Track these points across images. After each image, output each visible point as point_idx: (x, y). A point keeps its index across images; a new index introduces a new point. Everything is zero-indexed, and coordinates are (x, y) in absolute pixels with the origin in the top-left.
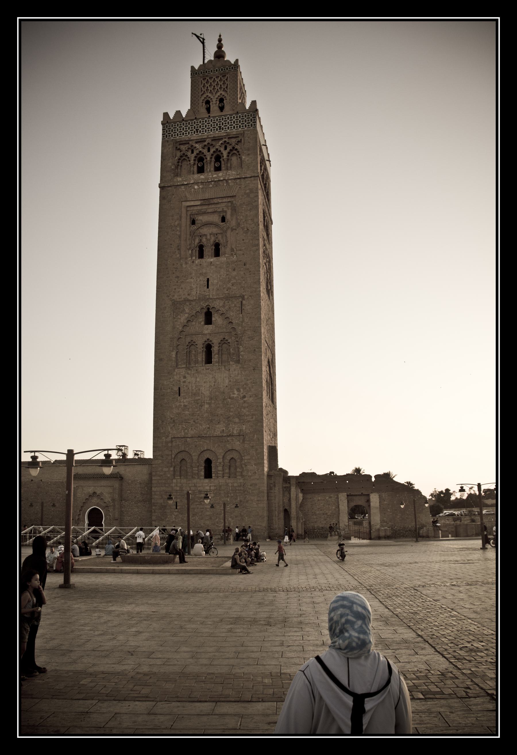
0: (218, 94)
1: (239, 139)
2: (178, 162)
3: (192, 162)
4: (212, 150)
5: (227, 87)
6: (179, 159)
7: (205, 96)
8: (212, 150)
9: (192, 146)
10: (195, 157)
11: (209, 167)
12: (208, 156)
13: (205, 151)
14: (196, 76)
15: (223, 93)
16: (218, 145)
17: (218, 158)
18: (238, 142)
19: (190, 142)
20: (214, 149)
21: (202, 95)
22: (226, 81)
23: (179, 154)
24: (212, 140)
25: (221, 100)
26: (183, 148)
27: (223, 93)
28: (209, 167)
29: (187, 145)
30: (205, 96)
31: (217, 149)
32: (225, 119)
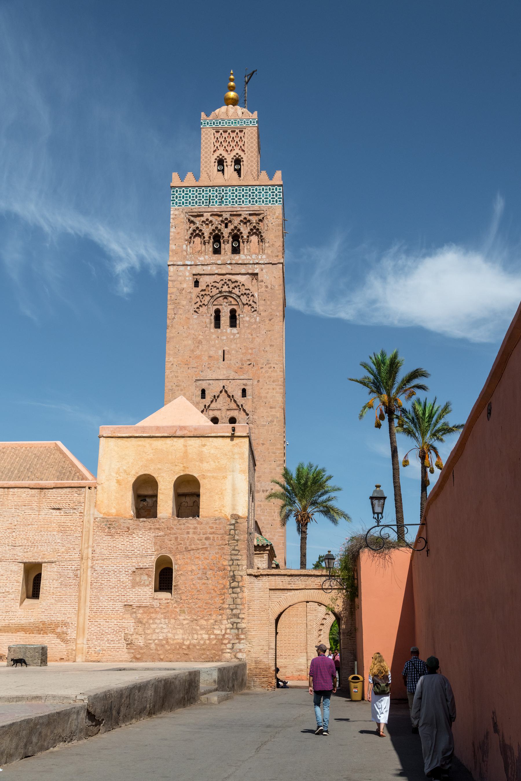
0: (234, 153)
1: (261, 217)
2: (190, 238)
3: (207, 238)
4: (231, 227)
5: (243, 145)
6: (192, 234)
7: (217, 154)
8: (231, 227)
9: (207, 220)
10: (211, 233)
11: (227, 248)
14: (208, 126)
15: (240, 153)
16: (236, 221)
17: (236, 237)
18: (260, 220)
19: (205, 214)
21: (214, 151)
22: (243, 138)
23: (193, 227)
24: (231, 215)
25: (238, 161)
26: (197, 220)
27: (240, 153)
28: (227, 248)
30: (217, 154)
31: (236, 227)
32: (246, 190)
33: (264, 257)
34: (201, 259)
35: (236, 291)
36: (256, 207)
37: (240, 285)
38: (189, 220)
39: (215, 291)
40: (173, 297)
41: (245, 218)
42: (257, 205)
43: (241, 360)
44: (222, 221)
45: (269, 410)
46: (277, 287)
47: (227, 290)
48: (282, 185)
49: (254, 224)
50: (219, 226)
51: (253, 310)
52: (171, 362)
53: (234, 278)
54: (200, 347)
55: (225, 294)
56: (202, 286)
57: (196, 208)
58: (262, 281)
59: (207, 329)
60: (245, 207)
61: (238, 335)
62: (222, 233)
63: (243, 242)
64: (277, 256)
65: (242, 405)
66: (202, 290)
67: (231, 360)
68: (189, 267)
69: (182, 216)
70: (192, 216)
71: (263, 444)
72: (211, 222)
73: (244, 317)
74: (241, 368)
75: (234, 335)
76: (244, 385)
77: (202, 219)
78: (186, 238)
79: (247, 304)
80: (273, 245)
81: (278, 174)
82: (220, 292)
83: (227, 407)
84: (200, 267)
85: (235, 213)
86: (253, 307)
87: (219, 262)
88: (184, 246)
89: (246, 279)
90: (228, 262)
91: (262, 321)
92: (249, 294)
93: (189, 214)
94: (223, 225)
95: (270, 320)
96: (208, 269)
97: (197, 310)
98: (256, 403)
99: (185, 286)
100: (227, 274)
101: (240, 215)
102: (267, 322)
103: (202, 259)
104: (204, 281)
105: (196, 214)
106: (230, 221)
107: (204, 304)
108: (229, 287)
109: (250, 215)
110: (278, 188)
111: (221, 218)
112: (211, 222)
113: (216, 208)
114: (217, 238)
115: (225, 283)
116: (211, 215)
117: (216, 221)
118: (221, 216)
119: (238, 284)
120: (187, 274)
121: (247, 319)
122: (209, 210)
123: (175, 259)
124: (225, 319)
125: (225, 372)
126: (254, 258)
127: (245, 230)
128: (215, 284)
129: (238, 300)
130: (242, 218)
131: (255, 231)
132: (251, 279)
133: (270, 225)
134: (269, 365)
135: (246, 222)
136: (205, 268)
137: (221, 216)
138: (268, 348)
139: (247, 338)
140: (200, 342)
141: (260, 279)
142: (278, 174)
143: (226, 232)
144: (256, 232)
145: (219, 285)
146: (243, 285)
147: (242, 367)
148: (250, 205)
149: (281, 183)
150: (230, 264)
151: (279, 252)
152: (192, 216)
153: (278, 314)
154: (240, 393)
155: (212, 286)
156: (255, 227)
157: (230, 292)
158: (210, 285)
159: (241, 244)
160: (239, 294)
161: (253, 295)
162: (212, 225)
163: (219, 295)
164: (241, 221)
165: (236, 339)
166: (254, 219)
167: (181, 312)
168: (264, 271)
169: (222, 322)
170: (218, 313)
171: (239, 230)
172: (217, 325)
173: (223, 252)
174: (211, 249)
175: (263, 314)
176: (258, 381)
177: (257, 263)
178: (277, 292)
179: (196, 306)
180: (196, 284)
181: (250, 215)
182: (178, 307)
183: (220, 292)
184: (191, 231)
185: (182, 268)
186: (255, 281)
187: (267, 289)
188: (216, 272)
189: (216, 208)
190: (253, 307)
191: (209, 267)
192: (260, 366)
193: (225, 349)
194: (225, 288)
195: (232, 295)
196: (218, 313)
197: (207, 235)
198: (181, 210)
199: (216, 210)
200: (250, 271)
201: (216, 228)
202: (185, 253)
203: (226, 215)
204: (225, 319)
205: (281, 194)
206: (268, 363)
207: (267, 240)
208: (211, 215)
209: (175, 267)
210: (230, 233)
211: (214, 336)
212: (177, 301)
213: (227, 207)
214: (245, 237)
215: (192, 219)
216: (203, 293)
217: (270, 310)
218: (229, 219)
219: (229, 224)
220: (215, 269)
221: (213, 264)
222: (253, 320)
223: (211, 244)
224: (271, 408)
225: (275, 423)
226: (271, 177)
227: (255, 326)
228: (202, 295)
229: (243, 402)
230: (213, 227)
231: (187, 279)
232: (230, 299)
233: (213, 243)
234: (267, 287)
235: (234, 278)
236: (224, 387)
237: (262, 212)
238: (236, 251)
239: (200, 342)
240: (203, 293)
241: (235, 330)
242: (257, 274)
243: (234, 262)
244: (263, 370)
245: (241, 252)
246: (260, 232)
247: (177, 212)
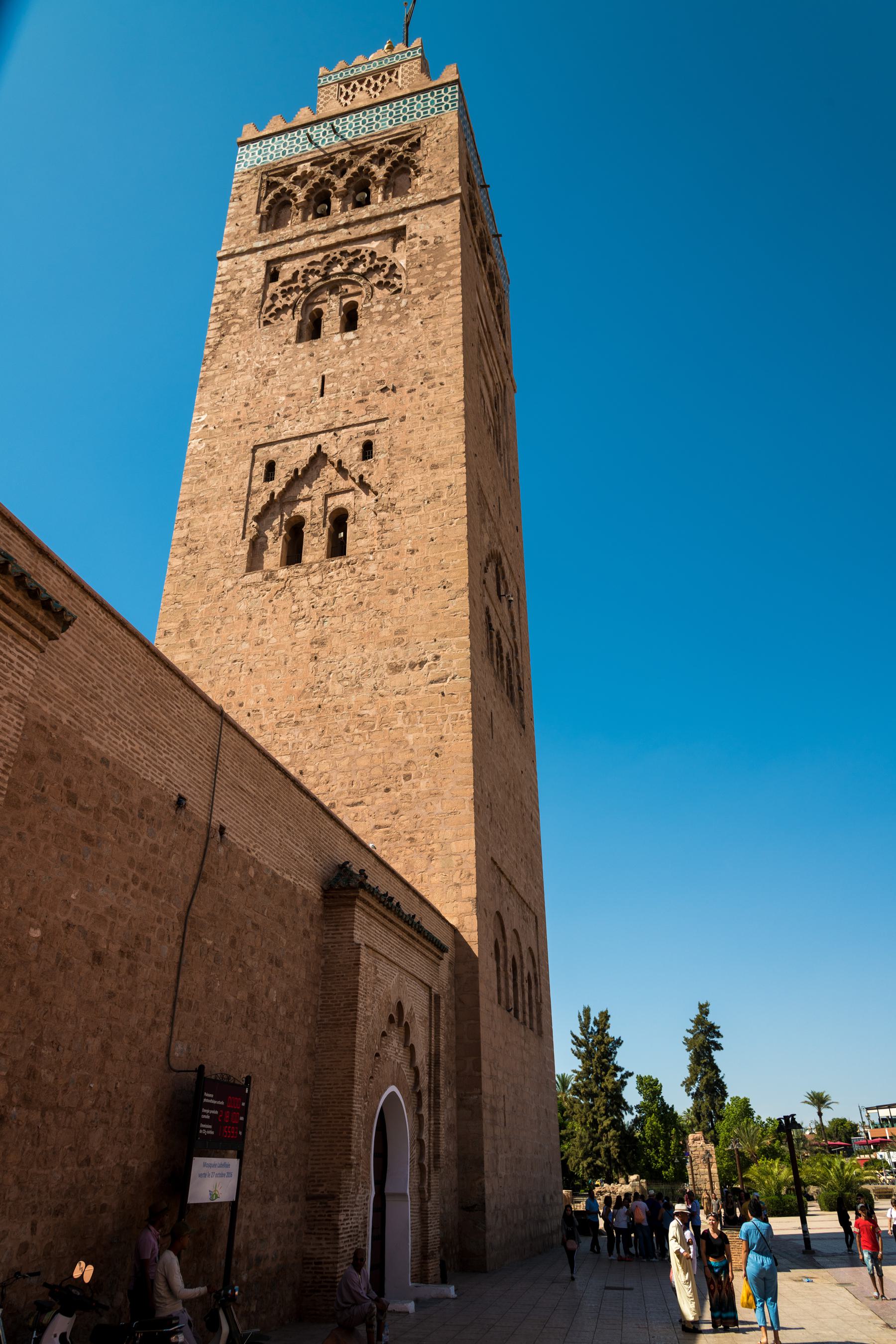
1: (415, 138)
13: (334, 178)
43: (363, 385)
45: (430, 472)
55: (334, 279)
58: (415, 236)
59: (288, 346)
61: (357, 342)
65: (361, 477)
66: (284, 284)
67: (338, 391)
71: (412, 552)
73: (372, 306)
74: (361, 401)
75: (349, 342)
76: (367, 433)
83: (326, 490)
95: (432, 298)
98: (397, 463)
102: (425, 301)
117: (322, 171)
121: (381, 307)
124: (331, 323)
125: (323, 418)
134: (431, 382)
138: (428, 351)
139: (377, 343)
145: (317, 267)
147: (366, 397)
153: (451, 283)
154: (357, 451)
164: (373, 157)
165: (353, 349)
175: (415, 291)
176: (403, 419)
181: (391, 142)
187: (424, 247)
192: (407, 388)
193: (325, 373)
201: (322, 180)
205: (457, 95)
206: (426, 379)
208: (312, 165)
210: (349, 181)
217: (432, 280)
224: (434, 467)
225: (445, 498)
227: (397, 316)
229: (365, 468)
236: (319, 447)
241: (350, 335)
244: (416, 395)
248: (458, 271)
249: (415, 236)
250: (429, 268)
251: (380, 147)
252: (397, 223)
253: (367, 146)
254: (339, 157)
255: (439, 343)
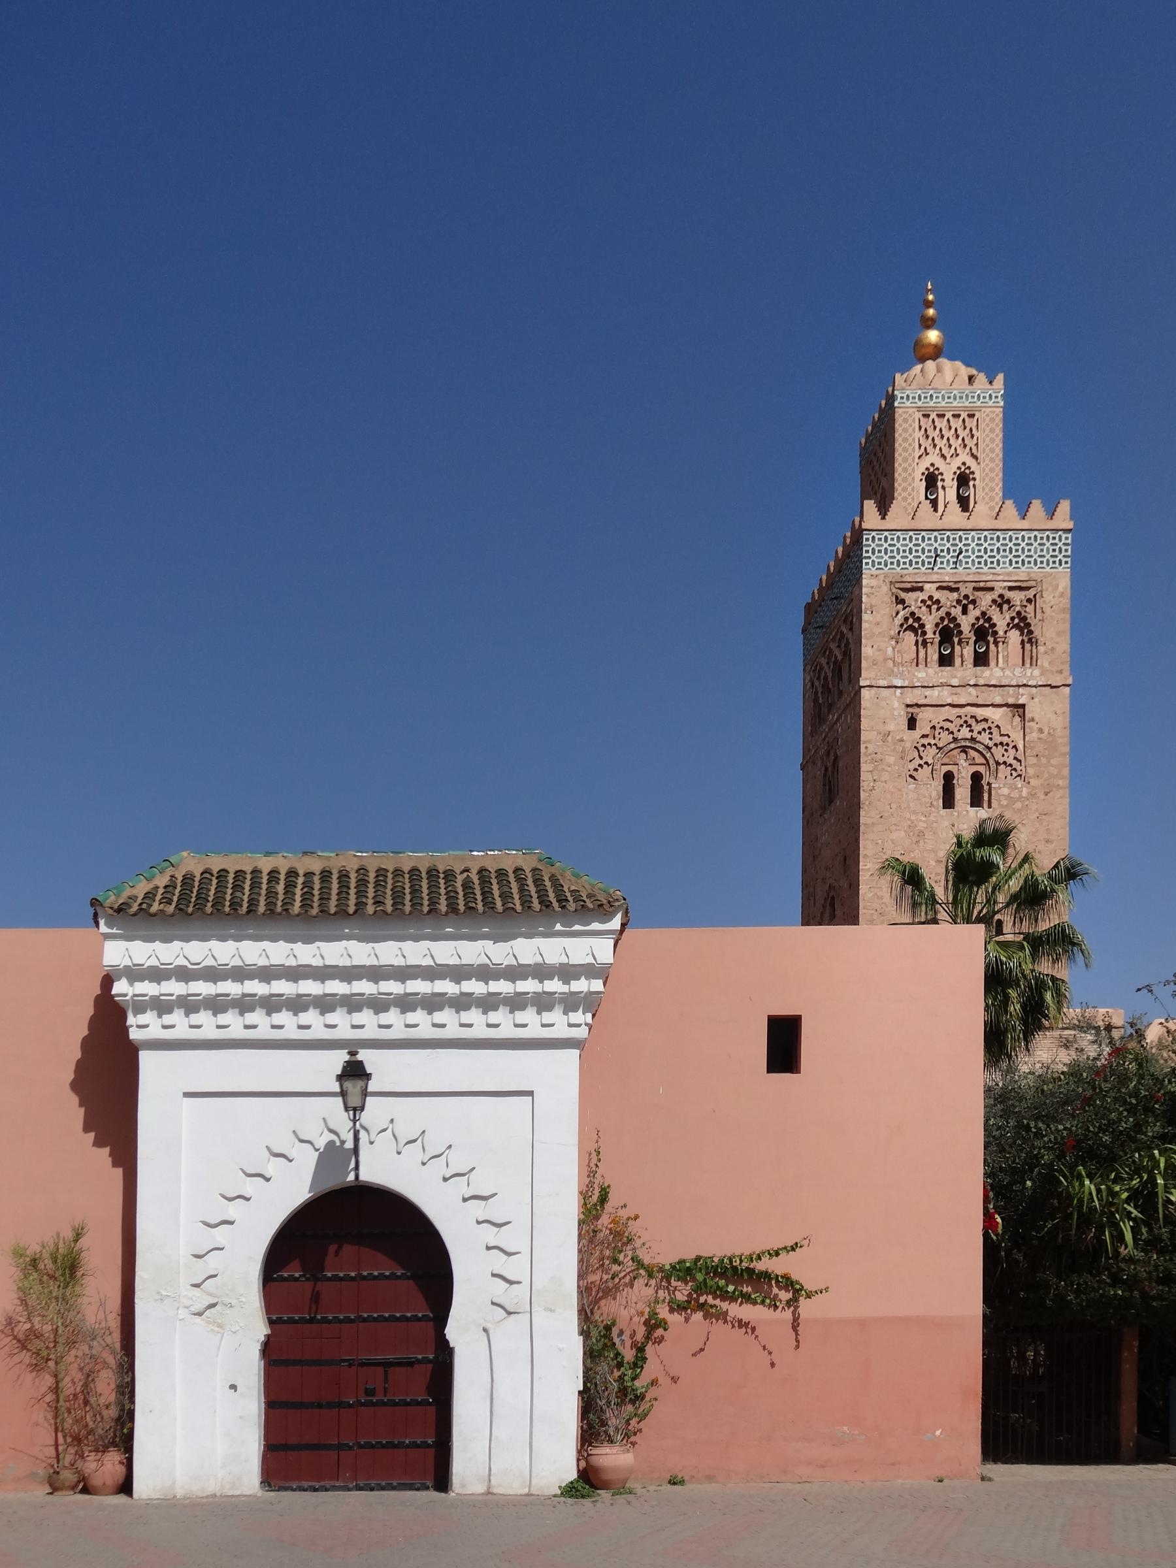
1: (1030, 594)
4: (974, 613)
6: (902, 625)
8: (974, 613)
9: (931, 598)
10: (937, 625)
12: (966, 628)
13: (957, 611)
16: (985, 599)
17: (984, 632)
18: (1029, 601)
19: (927, 586)
20: (977, 613)
24: (975, 589)
26: (910, 598)
29: (918, 593)
31: (984, 614)
32: (1004, 539)
33: (1037, 672)
34: (920, 675)
35: (984, 738)
36: (1022, 574)
37: (993, 726)
38: (897, 597)
39: (946, 738)
40: (871, 748)
41: (1001, 596)
42: (1023, 569)
44: (959, 602)
46: (1059, 732)
47: (968, 736)
48: (1069, 531)
49: (1018, 608)
50: (954, 612)
51: (1015, 774)
52: (868, 870)
53: (981, 712)
54: (921, 843)
55: (963, 744)
56: (923, 727)
57: (911, 575)
58: (1033, 720)
60: (1002, 573)
62: (959, 625)
63: (996, 643)
64: (1061, 672)
66: (924, 736)
68: (899, 691)
69: (885, 589)
70: (903, 590)
72: (938, 602)
77: (923, 596)
78: (892, 633)
79: (1005, 763)
80: (1053, 649)
81: (1065, 506)
82: (955, 740)
84: (918, 691)
85: (982, 585)
86: (1015, 770)
87: (955, 682)
88: (890, 650)
89: (1002, 716)
90: (972, 683)
91: (1033, 795)
92: (1007, 745)
93: (898, 585)
94: (960, 609)
96: (934, 695)
97: (914, 774)
99: (891, 727)
100: (968, 705)
101: (992, 589)
102: (1042, 797)
103: (922, 675)
104: (926, 717)
105: (909, 586)
106: (974, 602)
107: (926, 763)
108: (972, 731)
109: (1010, 589)
110: (1064, 536)
111: (955, 595)
112: (938, 602)
113: (946, 574)
114: (948, 634)
115: (966, 722)
116: (938, 588)
118: (957, 590)
119: (990, 724)
120: (896, 704)
121: (1005, 791)
122: (935, 578)
123: (873, 675)
124: (962, 792)
126: (1016, 674)
127: (1001, 621)
128: (947, 725)
129: (988, 755)
130: (994, 595)
131: (1016, 621)
132: (1010, 715)
133: (1047, 610)
135: (1002, 602)
136: (928, 692)
137: (957, 590)
140: (921, 834)
141: (1028, 715)
142: (1065, 506)
143: (966, 623)
144: (1022, 624)
146: (998, 726)
148: (1011, 569)
149: (1070, 525)
150: (975, 685)
151: (1063, 663)
152: (903, 590)
153: (1060, 782)
155: (942, 728)
156: (1019, 613)
157: (973, 739)
158: (938, 726)
159: (992, 647)
160: (991, 744)
161: (1015, 747)
162: (938, 609)
163: (953, 746)
164: (994, 601)
166: (1017, 597)
167: (885, 776)
168: (1036, 700)
169: (958, 796)
170: (949, 777)
171: (990, 619)
172: (948, 801)
173: (958, 661)
174: (936, 657)
175: (1033, 782)
177: (1025, 685)
178: (1060, 740)
179: (912, 766)
180: (912, 723)
181: (1010, 589)
182: (880, 767)
183: (955, 740)
184: (899, 619)
185: (886, 693)
186: (1017, 719)
188: (949, 701)
189: (947, 574)
190: (1015, 770)
191: (936, 692)
194: (965, 733)
195: (976, 746)
196: (949, 777)
197: (929, 628)
198: (882, 578)
199: (947, 579)
200: (1011, 701)
201: (948, 614)
202: (891, 663)
203: (966, 590)
204: (962, 792)
205: (1069, 548)
207: (1041, 640)
209: (873, 690)
211: (946, 823)
212: (879, 756)
213: (967, 572)
214: (1001, 633)
215: (903, 595)
216: (925, 741)
217: (1046, 776)
218: (971, 598)
219: (971, 607)
220: (946, 696)
221: (942, 685)
222: (1015, 794)
223: (936, 646)
226: (1051, 515)
228: (923, 745)
230: (942, 613)
231: (896, 713)
232: (972, 753)
233: (941, 644)
234: (1041, 731)
235: (981, 712)
237: (1033, 583)
238: (981, 660)
239: (921, 834)
240: (925, 741)
242: (1023, 706)
243: (982, 682)
245: (992, 663)
246: (1029, 625)
247: (874, 582)
248: (1066, 771)
249: (1033, 720)
250: (1044, 761)
251: (1001, 591)
252: (1018, 699)
253: (989, 585)
254: (964, 591)
255: (1052, 842)
